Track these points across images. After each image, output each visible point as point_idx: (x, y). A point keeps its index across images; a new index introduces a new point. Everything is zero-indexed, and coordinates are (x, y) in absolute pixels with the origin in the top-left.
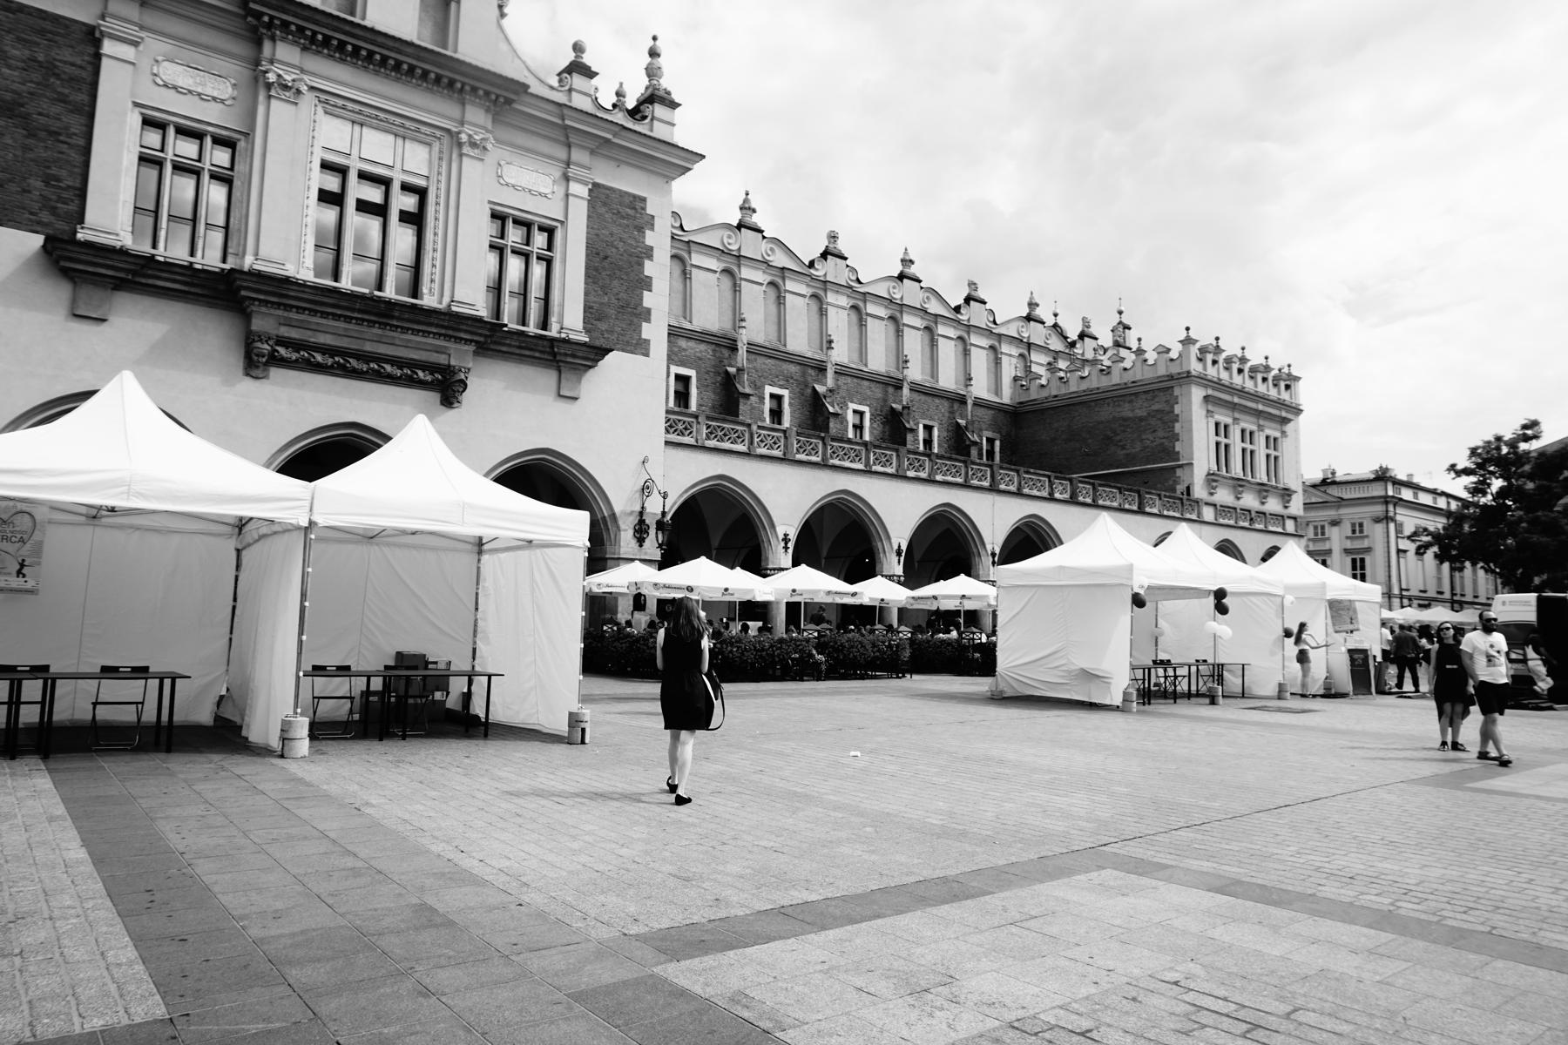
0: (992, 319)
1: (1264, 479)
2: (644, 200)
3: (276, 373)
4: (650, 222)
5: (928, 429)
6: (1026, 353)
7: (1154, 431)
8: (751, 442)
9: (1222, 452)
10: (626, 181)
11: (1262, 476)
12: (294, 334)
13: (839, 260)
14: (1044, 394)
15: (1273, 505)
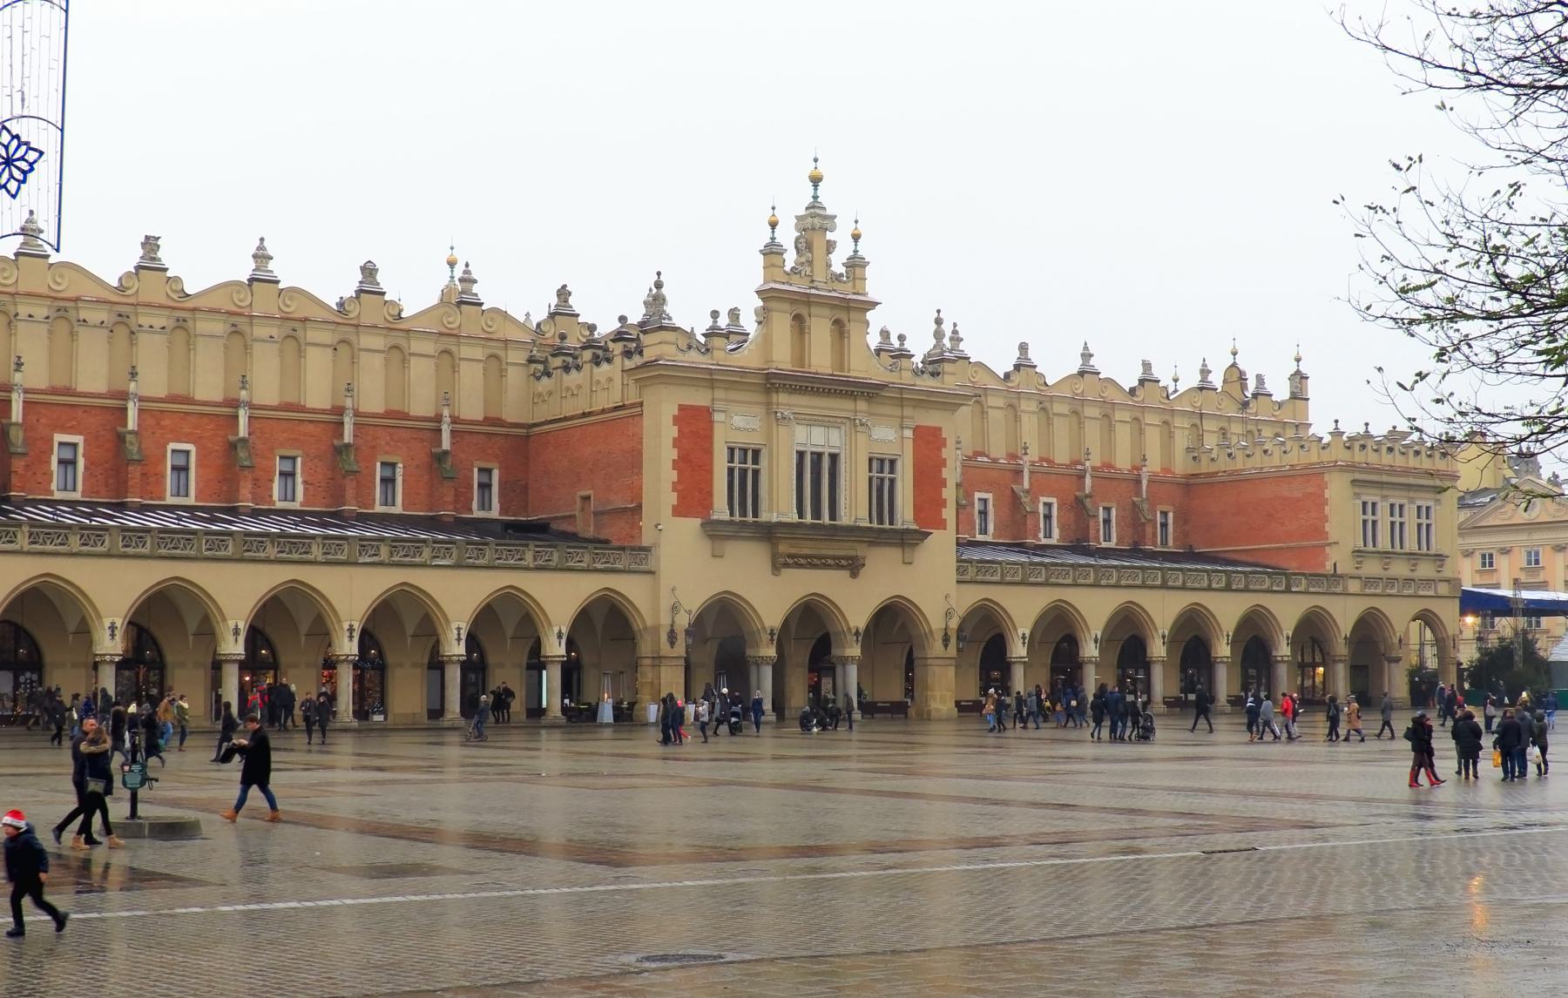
0: (1165, 395)
1: (1415, 548)
2: (940, 429)
3: (786, 572)
4: (943, 443)
5: (1107, 509)
6: (1198, 422)
7: (1308, 512)
8: (1002, 575)
9: (1369, 529)
10: (930, 419)
11: (1411, 544)
12: (793, 551)
13: (1028, 369)
14: (1213, 468)
15: (1425, 570)
